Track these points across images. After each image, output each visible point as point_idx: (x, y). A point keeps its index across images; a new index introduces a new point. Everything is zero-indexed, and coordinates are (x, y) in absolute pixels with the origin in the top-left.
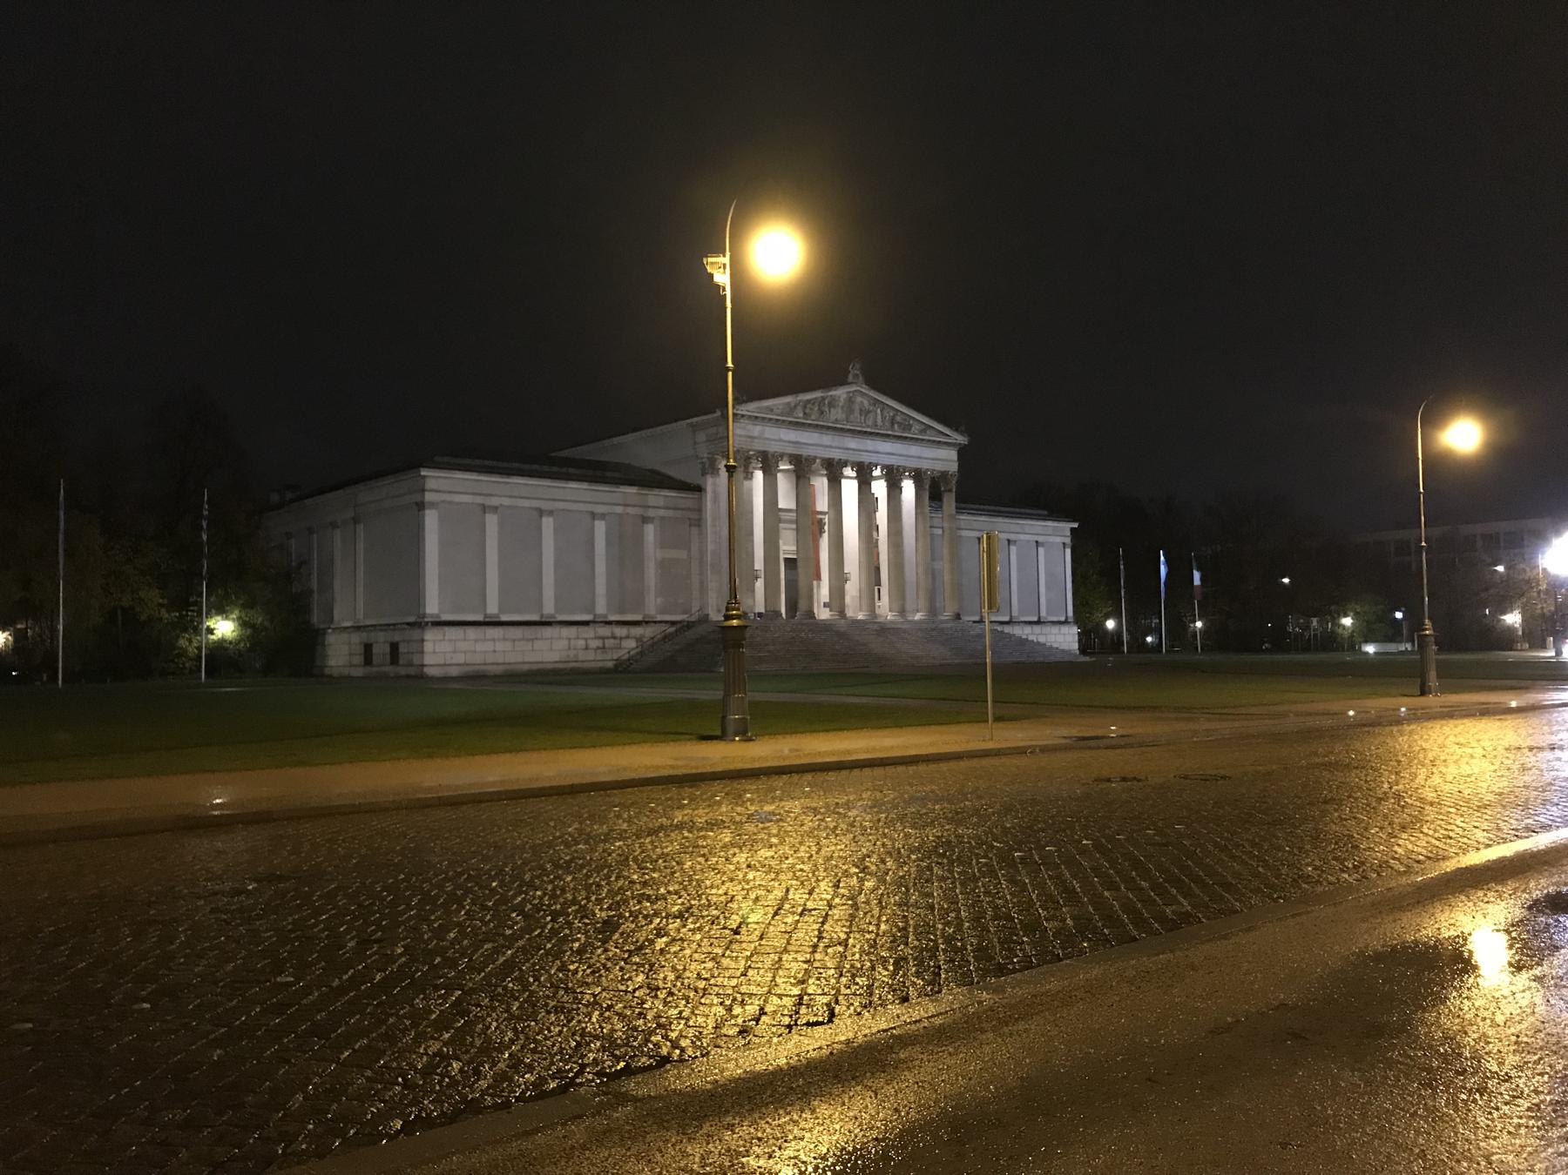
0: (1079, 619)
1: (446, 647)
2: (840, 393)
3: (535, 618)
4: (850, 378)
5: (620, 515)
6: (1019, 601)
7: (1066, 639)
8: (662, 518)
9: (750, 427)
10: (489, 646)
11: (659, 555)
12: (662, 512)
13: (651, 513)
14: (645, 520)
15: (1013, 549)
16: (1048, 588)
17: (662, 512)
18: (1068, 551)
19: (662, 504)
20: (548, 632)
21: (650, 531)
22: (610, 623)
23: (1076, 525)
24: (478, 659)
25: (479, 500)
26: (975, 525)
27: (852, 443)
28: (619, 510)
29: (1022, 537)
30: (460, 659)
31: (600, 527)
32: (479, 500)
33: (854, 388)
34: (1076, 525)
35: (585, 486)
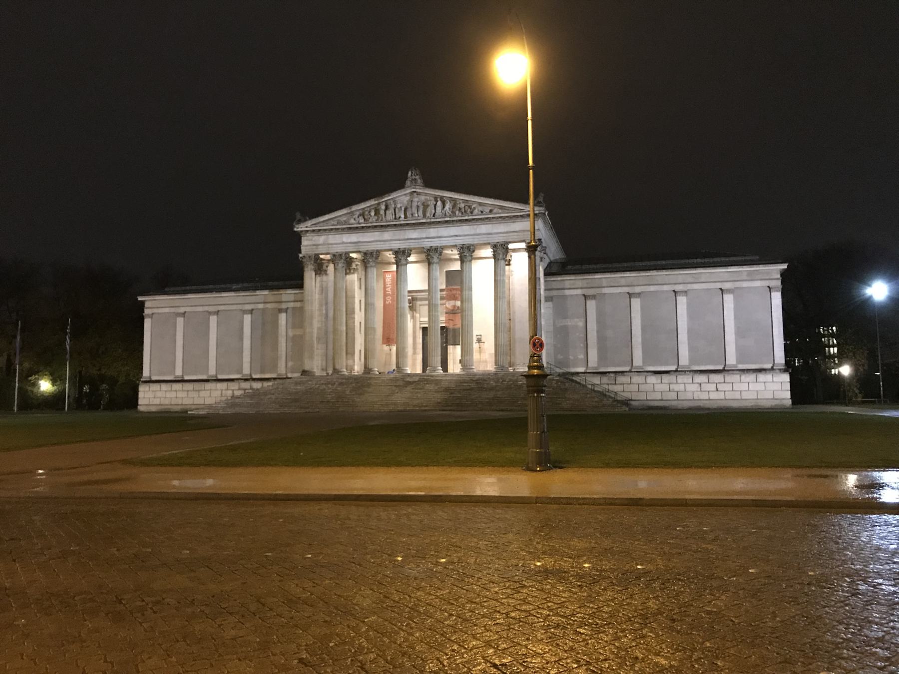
0: (789, 366)
1: (151, 395)
2: (401, 197)
3: (205, 377)
4: (408, 183)
5: (264, 310)
6: (691, 349)
7: (775, 389)
8: (294, 308)
9: (316, 238)
10: (173, 395)
11: (291, 334)
12: (291, 305)
13: (284, 306)
14: (280, 311)
15: (682, 300)
16: (740, 333)
17: (291, 305)
18: (777, 298)
19: (292, 299)
20: (208, 386)
21: (283, 317)
22: (254, 380)
23: (785, 266)
24: (167, 402)
25: (173, 310)
26: (623, 282)
27: (413, 234)
28: (261, 306)
29: (696, 286)
30: (157, 402)
31: (247, 318)
32: (173, 310)
33: (409, 191)
34: (785, 266)
35: (232, 294)
